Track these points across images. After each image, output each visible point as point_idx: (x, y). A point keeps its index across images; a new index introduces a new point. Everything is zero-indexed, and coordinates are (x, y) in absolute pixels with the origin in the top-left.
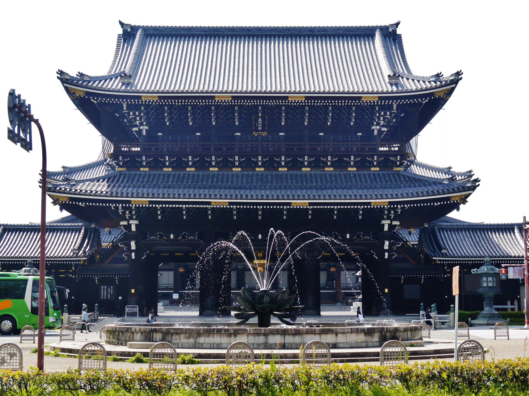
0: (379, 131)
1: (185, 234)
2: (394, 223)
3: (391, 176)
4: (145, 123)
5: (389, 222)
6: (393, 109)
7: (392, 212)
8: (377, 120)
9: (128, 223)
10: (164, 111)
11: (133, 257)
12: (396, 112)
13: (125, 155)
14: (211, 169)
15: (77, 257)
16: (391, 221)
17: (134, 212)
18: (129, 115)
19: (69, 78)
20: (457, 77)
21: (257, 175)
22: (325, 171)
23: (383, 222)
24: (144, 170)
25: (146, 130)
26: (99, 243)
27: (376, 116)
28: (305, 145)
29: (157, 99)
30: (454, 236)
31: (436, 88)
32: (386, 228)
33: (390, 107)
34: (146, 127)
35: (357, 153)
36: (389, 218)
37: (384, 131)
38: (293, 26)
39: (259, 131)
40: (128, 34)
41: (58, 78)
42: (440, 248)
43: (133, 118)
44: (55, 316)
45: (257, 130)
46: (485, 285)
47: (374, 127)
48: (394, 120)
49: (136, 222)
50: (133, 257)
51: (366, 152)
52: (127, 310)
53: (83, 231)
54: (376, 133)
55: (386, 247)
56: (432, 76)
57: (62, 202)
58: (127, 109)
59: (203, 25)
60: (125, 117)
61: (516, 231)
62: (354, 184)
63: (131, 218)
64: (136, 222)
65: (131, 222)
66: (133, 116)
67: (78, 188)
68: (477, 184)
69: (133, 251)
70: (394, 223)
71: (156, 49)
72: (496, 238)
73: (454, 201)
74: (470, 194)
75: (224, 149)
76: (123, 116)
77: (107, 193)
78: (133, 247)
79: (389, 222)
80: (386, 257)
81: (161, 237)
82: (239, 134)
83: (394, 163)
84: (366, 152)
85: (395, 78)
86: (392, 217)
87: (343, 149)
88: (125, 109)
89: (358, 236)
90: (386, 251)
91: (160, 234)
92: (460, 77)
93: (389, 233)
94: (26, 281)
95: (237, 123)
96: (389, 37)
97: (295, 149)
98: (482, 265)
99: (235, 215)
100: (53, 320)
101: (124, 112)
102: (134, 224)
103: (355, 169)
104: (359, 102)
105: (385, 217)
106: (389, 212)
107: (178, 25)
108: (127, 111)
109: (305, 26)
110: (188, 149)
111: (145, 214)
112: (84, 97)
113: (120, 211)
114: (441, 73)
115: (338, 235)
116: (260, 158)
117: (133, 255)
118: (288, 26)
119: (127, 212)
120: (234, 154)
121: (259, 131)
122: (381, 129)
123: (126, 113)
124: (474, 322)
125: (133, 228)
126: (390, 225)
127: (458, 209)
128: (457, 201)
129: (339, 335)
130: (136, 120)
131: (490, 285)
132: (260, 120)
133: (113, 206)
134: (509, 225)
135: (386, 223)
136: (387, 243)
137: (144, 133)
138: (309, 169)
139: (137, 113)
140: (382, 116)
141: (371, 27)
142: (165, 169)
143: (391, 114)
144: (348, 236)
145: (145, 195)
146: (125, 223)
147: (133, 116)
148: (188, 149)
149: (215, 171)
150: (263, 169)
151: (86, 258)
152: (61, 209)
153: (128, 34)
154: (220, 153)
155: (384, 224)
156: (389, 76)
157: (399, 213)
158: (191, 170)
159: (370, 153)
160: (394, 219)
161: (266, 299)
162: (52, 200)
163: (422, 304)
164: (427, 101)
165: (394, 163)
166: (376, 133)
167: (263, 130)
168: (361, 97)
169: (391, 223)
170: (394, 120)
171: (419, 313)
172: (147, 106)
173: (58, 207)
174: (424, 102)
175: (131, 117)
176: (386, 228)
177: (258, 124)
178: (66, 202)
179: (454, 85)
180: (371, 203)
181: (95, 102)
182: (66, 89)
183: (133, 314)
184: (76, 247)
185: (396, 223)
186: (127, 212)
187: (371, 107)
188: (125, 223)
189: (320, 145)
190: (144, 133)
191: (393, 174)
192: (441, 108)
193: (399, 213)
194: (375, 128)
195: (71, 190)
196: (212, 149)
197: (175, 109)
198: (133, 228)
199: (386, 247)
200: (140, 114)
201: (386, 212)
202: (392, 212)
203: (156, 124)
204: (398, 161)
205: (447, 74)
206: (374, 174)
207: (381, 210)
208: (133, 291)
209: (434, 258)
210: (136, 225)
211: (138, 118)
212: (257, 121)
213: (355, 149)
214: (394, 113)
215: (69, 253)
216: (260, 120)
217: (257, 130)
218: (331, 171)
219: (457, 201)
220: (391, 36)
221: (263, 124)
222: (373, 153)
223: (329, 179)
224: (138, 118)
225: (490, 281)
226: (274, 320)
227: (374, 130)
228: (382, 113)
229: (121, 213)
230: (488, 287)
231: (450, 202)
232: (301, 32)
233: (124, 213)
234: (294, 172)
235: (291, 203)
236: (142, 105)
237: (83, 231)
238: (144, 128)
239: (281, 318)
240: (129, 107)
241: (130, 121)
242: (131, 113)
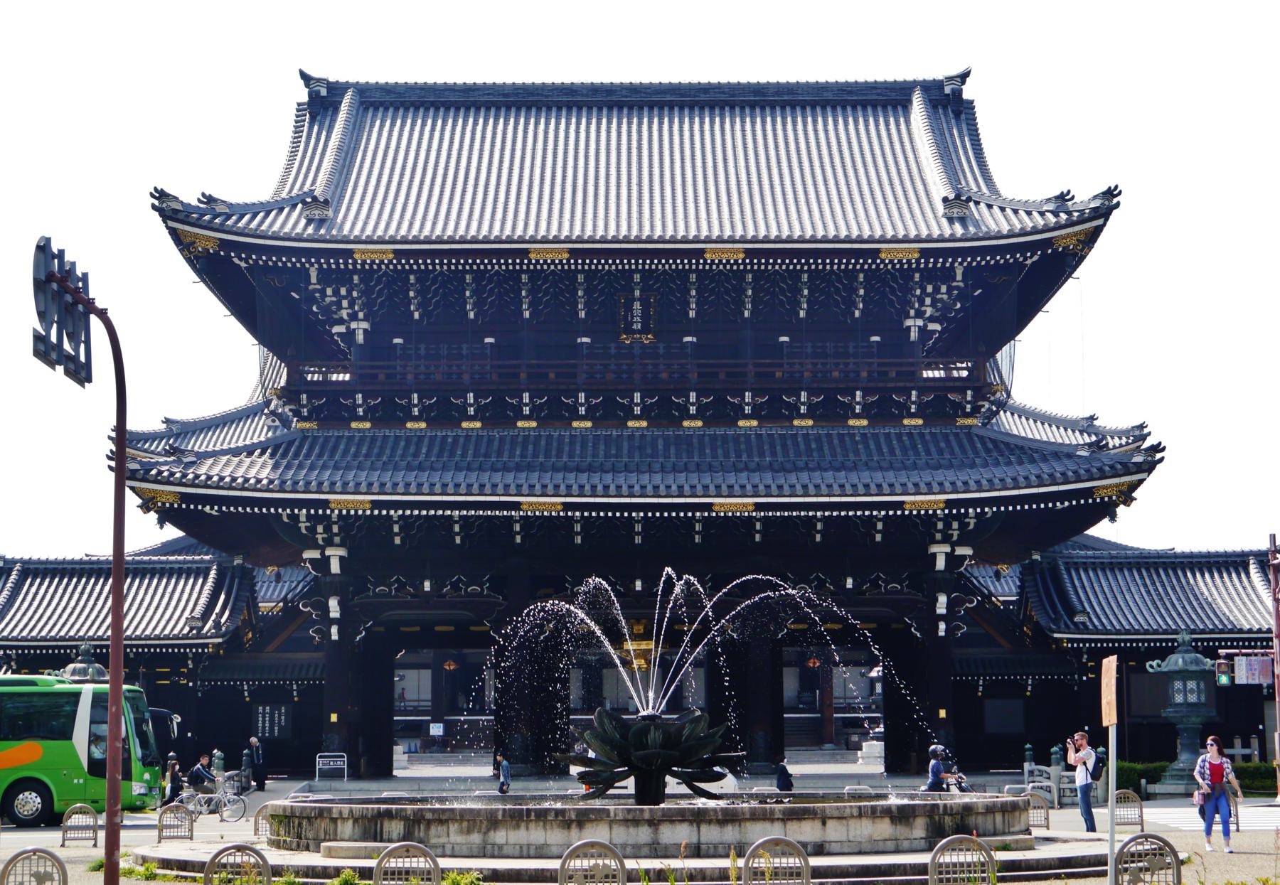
0: (923, 330)
1: (459, 580)
3: (952, 438)
4: (361, 315)
6: (954, 280)
7: (955, 525)
8: (917, 305)
9: (323, 554)
10: (406, 287)
11: (335, 637)
12: (961, 284)
13: (315, 390)
14: (520, 424)
15: (198, 636)
16: (953, 546)
17: (335, 529)
18: (323, 292)
19: (180, 208)
20: (1108, 203)
21: (631, 437)
22: (793, 426)
23: (934, 549)
24: (361, 426)
25: (365, 331)
26: (253, 603)
27: (914, 296)
28: (746, 365)
29: (391, 256)
31: (1058, 227)
32: (941, 564)
33: (948, 275)
34: (365, 325)
35: (872, 385)
36: (946, 539)
37: (934, 332)
38: (714, 80)
39: (635, 332)
40: (321, 101)
41: (154, 207)
42: (1072, 612)
43: (332, 303)
44: (147, 781)
45: (629, 330)
46: (1179, 699)
47: (909, 322)
48: (959, 305)
49: (342, 552)
50: (335, 637)
51: (892, 380)
52: (320, 763)
53: (213, 574)
54: (914, 335)
55: (941, 609)
56: (1048, 200)
57: (164, 504)
58: (319, 282)
59: (499, 81)
60: (314, 300)
61: (1253, 569)
62: (864, 458)
63: (329, 542)
64: (342, 552)
67: (202, 470)
68: (1158, 456)
69: (334, 621)
71: (388, 138)
72: (1205, 585)
73: (1102, 499)
74: (1141, 482)
75: (552, 376)
76: (311, 299)
77: (271, 482)
78: (335, 612)
79: (948, 549)
80: (942, 633)
81: (402, 586)
82: (585, 340)
84: (892, 380)
85: (958, 203)
86: (955, 538)
87: (836, 374)
88: (314, 280)
89: (875, 584)
90: (942, 617)
91: (398, 581)
92: (1115, 201)
93: (948, 575)
94: (76, 696)
95: (582, 314)
96: (945, 108)
97: (722, 376)
98: (1172, 650)
99: (578, 534)
100: (143, 791)
101: (311, 287)
102: (335, 555)
103: (865, 422)
104: (874, 262)
105: (938, 536)
106: (948, 526)
107: (440, 81)
108: (318, 287)
109: (744, 80)
110: (466, 377)
111: (363, 534)
113: (302, 526)
114: (1069, 192)
115: (824, 582)
116: (637, 397)
117: (334, 630)
118: (704, 80)
119: (320, 529)
120: (573, 387)
121: (635, 332)
122: (925, 326)
123: (315, 290)
124: (1154, 788)
125: (335, 567)
126: (950, 557)
127: (1113, 518)
128: (1110, 497)
129: (830, 823)
130: (340, 308)
131: (1192, 698)
132: (637, 306)
133: (285, 513)
134: (1235, 554)
135: (940, 552)
137: (360, 338)
138: (755, 423)
139: (343, 291)
140: (928, 295)
141: (901, 83)
142: (409, 425)
143: (950, 289)
144: (849, 583)
145: (363, 487)
146: (315, 554)
148: (466, 377)
149: (529, 429)
150: (644, 424)
151: (220, 640)
152: (161, 523)
153: (321, 101)
154: (542, 387)
155: (934, 555)
156: (945, 200)
157: (971, 527)
159: (901, 384)
160: (961, 542)
161: (654, 736)
162: (140, 501)
163: (1028, 746)
164: (1035, 258)
165: (958, 409)
166: (914, 335)
167: (645, 330)
168: (878, 251)
169: (953, 550)
170: (959, 305)
171: (1022, 768)
172: (368, 274)
173: (153, 516)
174: (1029, 262)
175: (328, 300)
176: (941, 564)
177: (633, 317)
178: (172, 505)
179: (1100, 221)
180: (903, 502)
181: (243, 264)
182: (174, 233)
183: (335, 774)
184: (197, 614)
185: (965, 551)
186: (320, 529)
187: (904, 273)
188: (315, 554)
189: (781, 365)
190: (360, 338)
191: (957, 435)
192: (1069, 276)
193: (971, 527)
194: (913, 324)
195: (184, 476)
196: (523, 376)
197: (434, 281)
198: (335, 567)
199: (941, 609)
200: (349, 292)
201: (940, 525)
202: (955, 525)
203: (387, 316)
204: (968, 402)
205: (1085, 194)
206: (910, 435)
207: (929, 520)
208: (334, 718)
209: (1056, 635)
210: (341, 558)
211: (345, 303)
213: (864, 374)
214: (957, 288)
215: (181, 628)
216: (637, 305)
217: (629, 330)
218: (807, 427)
219: (1110, 497)
220: (949, 104)
221: (645, 316)
223: (802, 447)
224: (345, 303)
225: (1192, 691)
226: (673, 785)
227: (909, 328)
228: (930, 289)
229: (304, 531)
230: (1187, 704)
231: (1094, 500)
232: (734, 95)
233: (312, 530)
234: (720, 431)
235: (711, 504)
236: (355, 271)
237: (213, 574)
238: (361, 327)
239: (688, 780)
240: (325, 277)
241: (326, 310)
242: (329, 291)
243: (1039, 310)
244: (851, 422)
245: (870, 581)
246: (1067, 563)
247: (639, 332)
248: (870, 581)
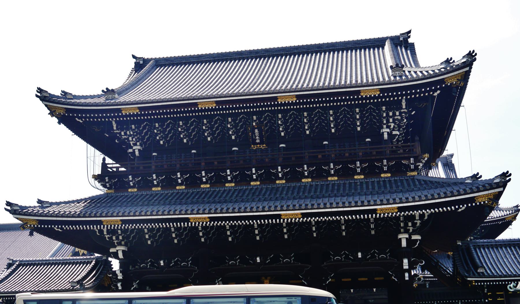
1: (178, 259)
2: (414, 237)
3: (405, 181)
5: (407, 236)
12: (406, 110)
17: (121, 238)
18: (120, 133)
20: (471, 57)
23: (400, 236)
25: (139, 150)
28: (305, 153)
29: (138, 111)
30: (492, 253)
32: (404, 244)
34: (139, 147)
36: (406, 231)
38: (301, 44)
42: (476, 267)
45: (255, 143)
47: (384, 130)
51: (374, 156)
58: (117, 129)
62: (359, 191)
63: (120, 244)
65: (118, 248)
66: (125, 137)
69: (120, 281)
70: (414, 237)
75: (216, 163)
76: (114, 136)
79: (407, 236)
83: (408, 168)
84: (374, 156)
85: (398, 67)
86: (411, 231)
87: (347, 155)
88: (115, 128)
89: (373, 256)
97: (293, 159)
103: (362, 177)
105: (402, 230)
106: (406, 225)
107: (188, 54)
108: (117, 131)
112: (64, 115)
113: (107, 236)
115: (349, 255)
119: (114, 238)
126: (408, 240)
128: (484, 202)
132: (256, 131)
135: (403, 237)
136: (406, 261)
137: (137, 153)
138: (310, 180)
140: (391, 117)
141: (381, 38)
143: (401, 114)
147: (125, 137)
148: (178, 166)
149: (206, 188)
156: (391, 67)
157: (418, 224)
158: (181, 188)
159: (379, 157)
160: (415, 232)
165: (408, 168)
167: (261, 143)
169: (410, 237)
175: (123, 137)
176: (404, 244)
177: (255, 136)
178: (34, 226)
186: (114, 238)
190: (137, 153)
191: (407, 180)
193: (418, 224)
194: (385, 131)
196: (203, 164)
204: (412, 164)
209: (468, 279)
212: (254, 133)
214: (404, 112)
216: (256, 131)
217: (255, 143)
219: (484, 202)
221: (261, 136)
222: (382, 157)
224: (130, 139)
227: (383, 133)
228: (391, 114)
232: (309, 49)
233: (111, 238)
242: (123, 133)
243: (451, 130)
244: (356, 177)
245: (371, 254)
246: (474, 246)
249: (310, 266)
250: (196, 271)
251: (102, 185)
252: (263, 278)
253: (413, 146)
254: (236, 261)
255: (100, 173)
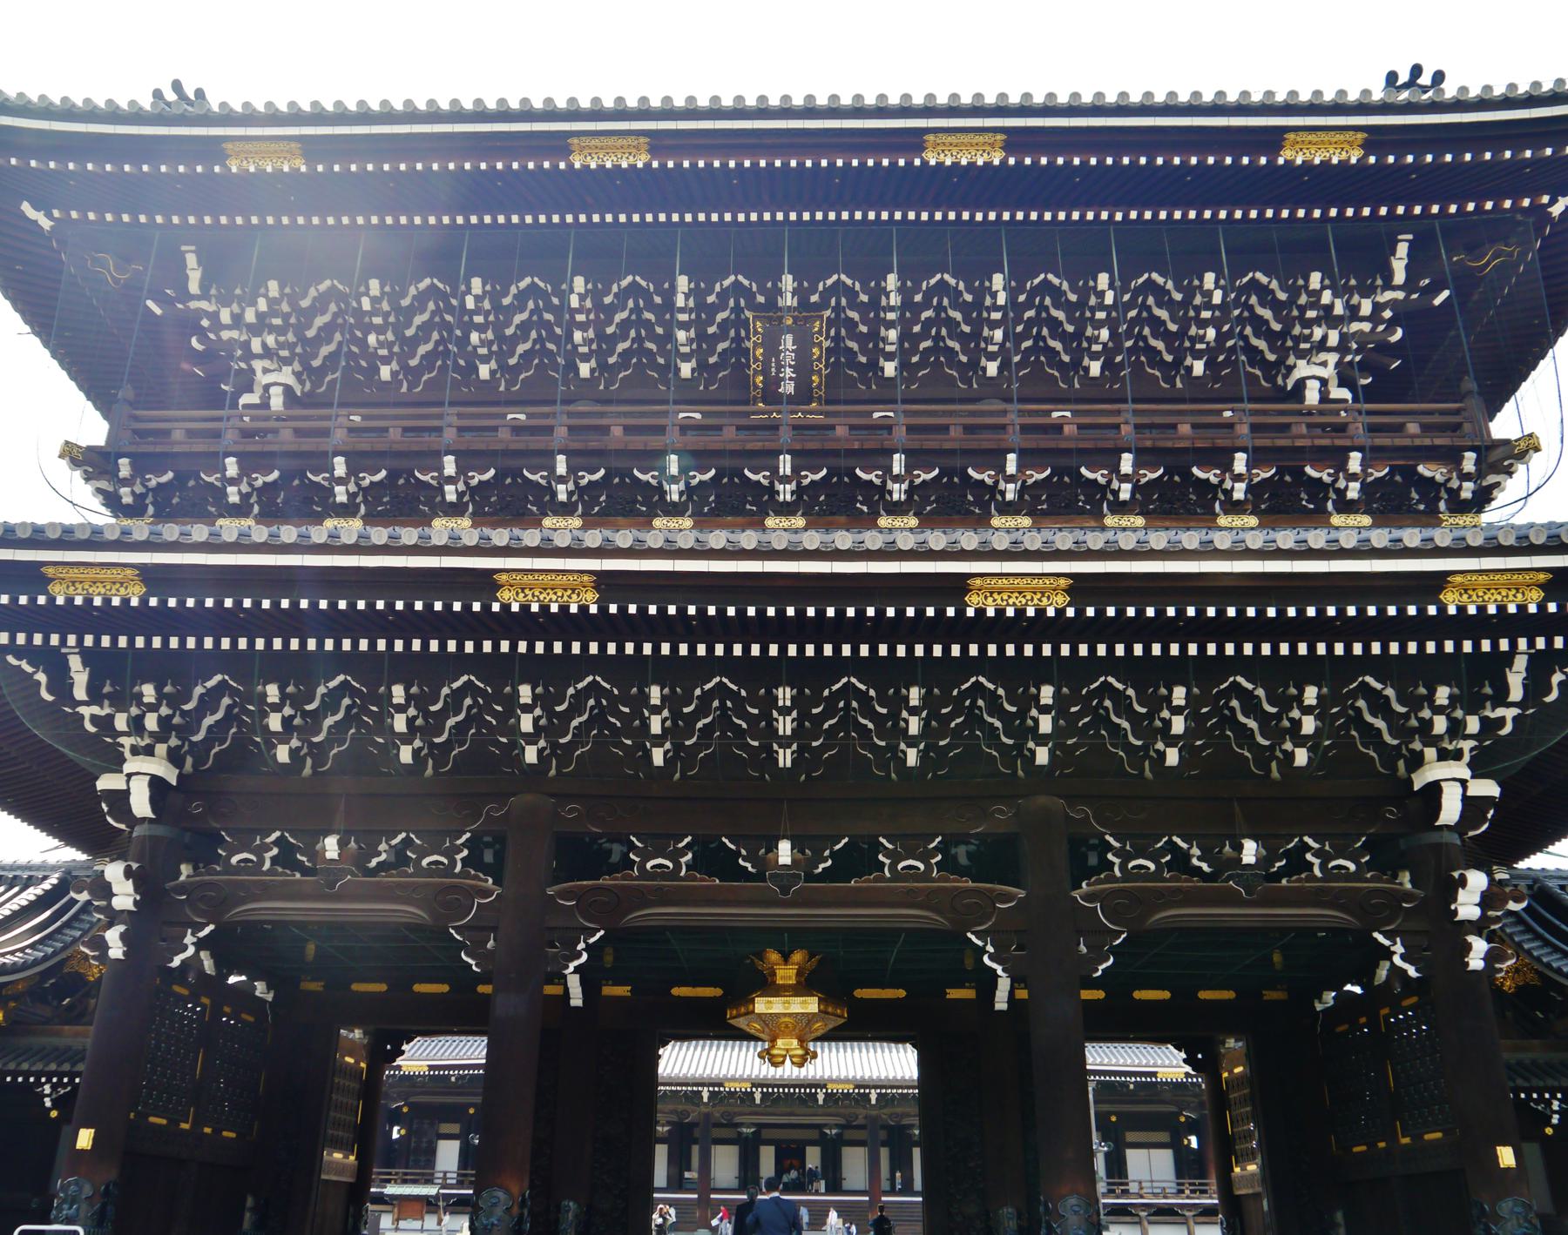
1: (408, 842)
7: (1473, 725)
32: (1451, 810)
81: (286, 858)
89: (1297, 863)
105: (1430, 753)
123: (202, 313)
144: (1250, 851)
155: (1434, 789)
157: (1508, 728)
193: (1508, 728)
196: (561, 432)
201: (1440, 725)
247: (791, 400)
248: (1287, 854)
249: (1022, 894)
250: (486, 893)
251: (99, 491)
252: (774, 956)
253: (1457, 412)
254: (675, 856)
255: (102, 443)
